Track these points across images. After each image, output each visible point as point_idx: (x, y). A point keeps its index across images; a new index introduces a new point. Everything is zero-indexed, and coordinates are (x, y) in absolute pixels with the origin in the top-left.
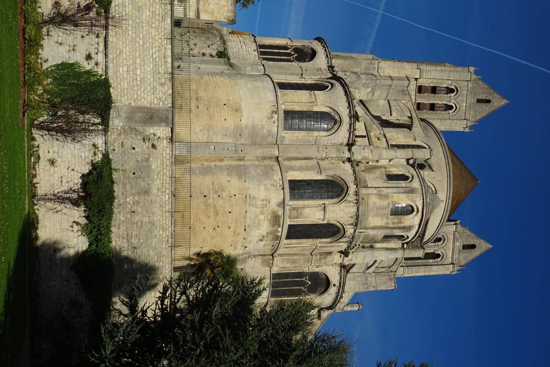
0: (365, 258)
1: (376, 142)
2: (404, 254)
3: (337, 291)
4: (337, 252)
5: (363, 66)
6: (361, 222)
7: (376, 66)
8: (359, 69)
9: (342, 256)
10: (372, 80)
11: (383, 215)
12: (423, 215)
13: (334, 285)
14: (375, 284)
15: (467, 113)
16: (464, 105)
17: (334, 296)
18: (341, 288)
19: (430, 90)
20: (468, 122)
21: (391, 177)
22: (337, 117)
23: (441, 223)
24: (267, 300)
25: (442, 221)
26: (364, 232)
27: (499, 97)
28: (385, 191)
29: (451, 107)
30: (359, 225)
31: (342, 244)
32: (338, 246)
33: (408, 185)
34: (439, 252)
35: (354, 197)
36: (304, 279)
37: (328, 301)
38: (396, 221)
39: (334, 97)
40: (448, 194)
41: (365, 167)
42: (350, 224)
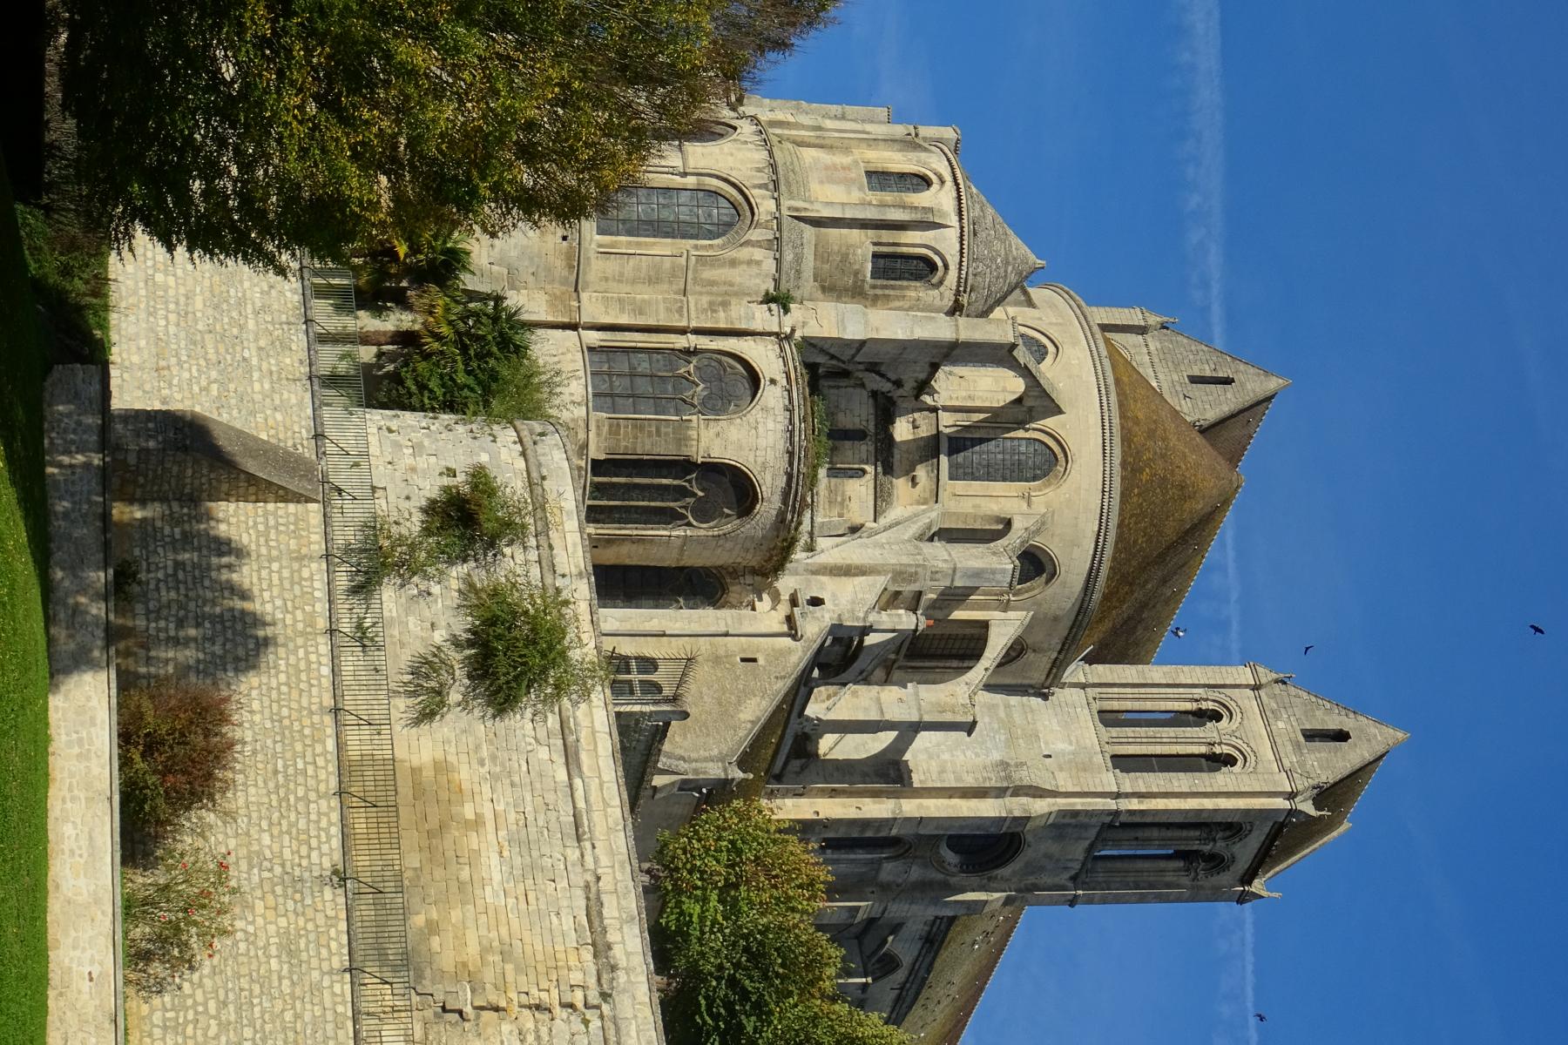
0: (843, 320)
2: (957, 326)
3: (787, 402)
4: (761, 303)
6: (788, 184)
9: (774, 306)
11: (848, 182)
12: (957, 184)
13: (773, 382)
14: (947, 557)
17: (782, 417)
18: (794, 384)
23: (1107, 431)
24: (584, 408)
25: (1107, 424)
26: (805, 209)
27: (1252, 370)
30: (783, 188)
31: (758, 254)
32: (750, 262)
34: (1226, 750)
35: (757, 138)
36: (682, 371)
37: (771, 440)
40: (1094, 349)
42: (760, 186)
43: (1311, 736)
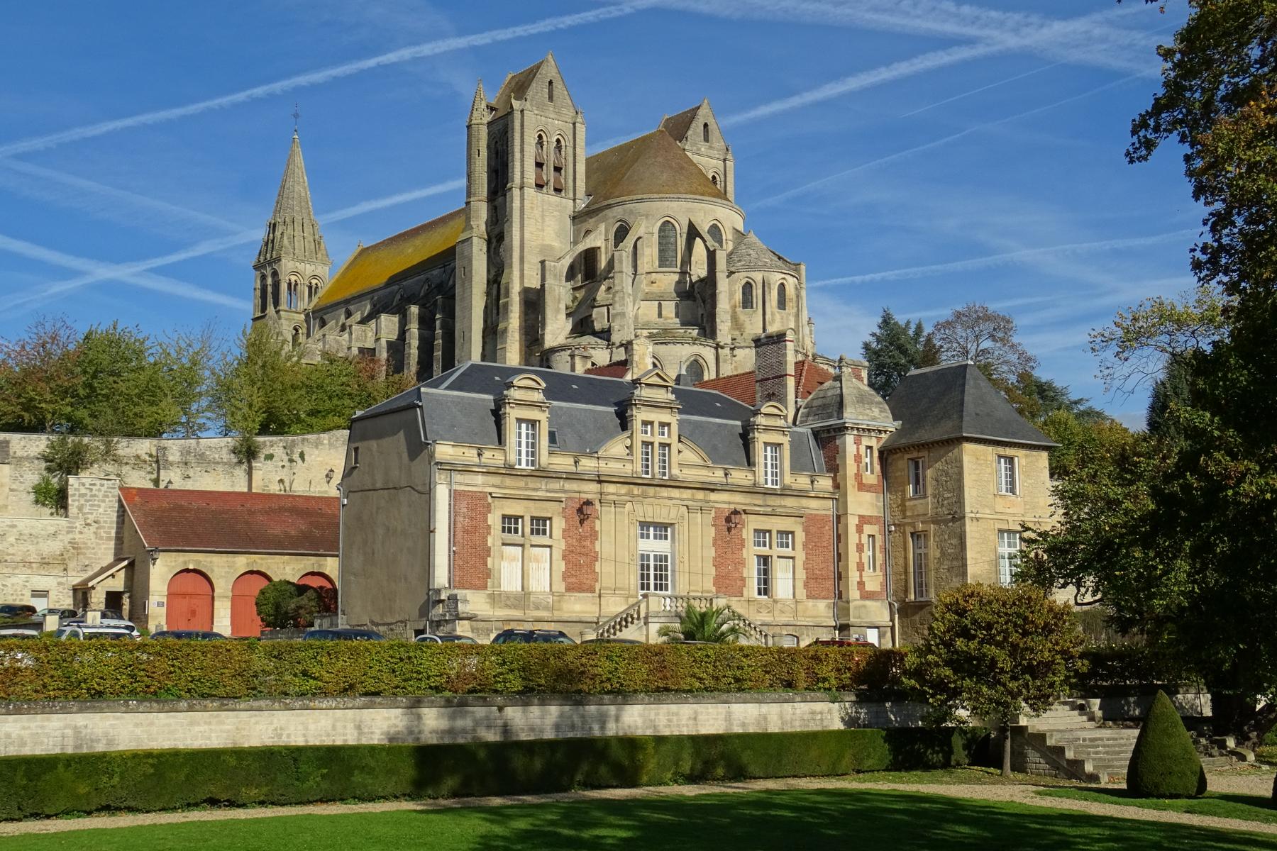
1: (658, 287)
5: (552, 282)
7: (553, 264)
8: (556, 287)
10: (623, 298)
15: (564, 119)
16: (556, 122)
19: (540, 169)
20: (578, 120)
21: (747, 302)
22: (692, 359)
28: (768, 316)
29: (558, 141)
33: (760, 286)
38: (791, 304)
39: (670, 358)
41: (734, 329)
43: (706, 139)
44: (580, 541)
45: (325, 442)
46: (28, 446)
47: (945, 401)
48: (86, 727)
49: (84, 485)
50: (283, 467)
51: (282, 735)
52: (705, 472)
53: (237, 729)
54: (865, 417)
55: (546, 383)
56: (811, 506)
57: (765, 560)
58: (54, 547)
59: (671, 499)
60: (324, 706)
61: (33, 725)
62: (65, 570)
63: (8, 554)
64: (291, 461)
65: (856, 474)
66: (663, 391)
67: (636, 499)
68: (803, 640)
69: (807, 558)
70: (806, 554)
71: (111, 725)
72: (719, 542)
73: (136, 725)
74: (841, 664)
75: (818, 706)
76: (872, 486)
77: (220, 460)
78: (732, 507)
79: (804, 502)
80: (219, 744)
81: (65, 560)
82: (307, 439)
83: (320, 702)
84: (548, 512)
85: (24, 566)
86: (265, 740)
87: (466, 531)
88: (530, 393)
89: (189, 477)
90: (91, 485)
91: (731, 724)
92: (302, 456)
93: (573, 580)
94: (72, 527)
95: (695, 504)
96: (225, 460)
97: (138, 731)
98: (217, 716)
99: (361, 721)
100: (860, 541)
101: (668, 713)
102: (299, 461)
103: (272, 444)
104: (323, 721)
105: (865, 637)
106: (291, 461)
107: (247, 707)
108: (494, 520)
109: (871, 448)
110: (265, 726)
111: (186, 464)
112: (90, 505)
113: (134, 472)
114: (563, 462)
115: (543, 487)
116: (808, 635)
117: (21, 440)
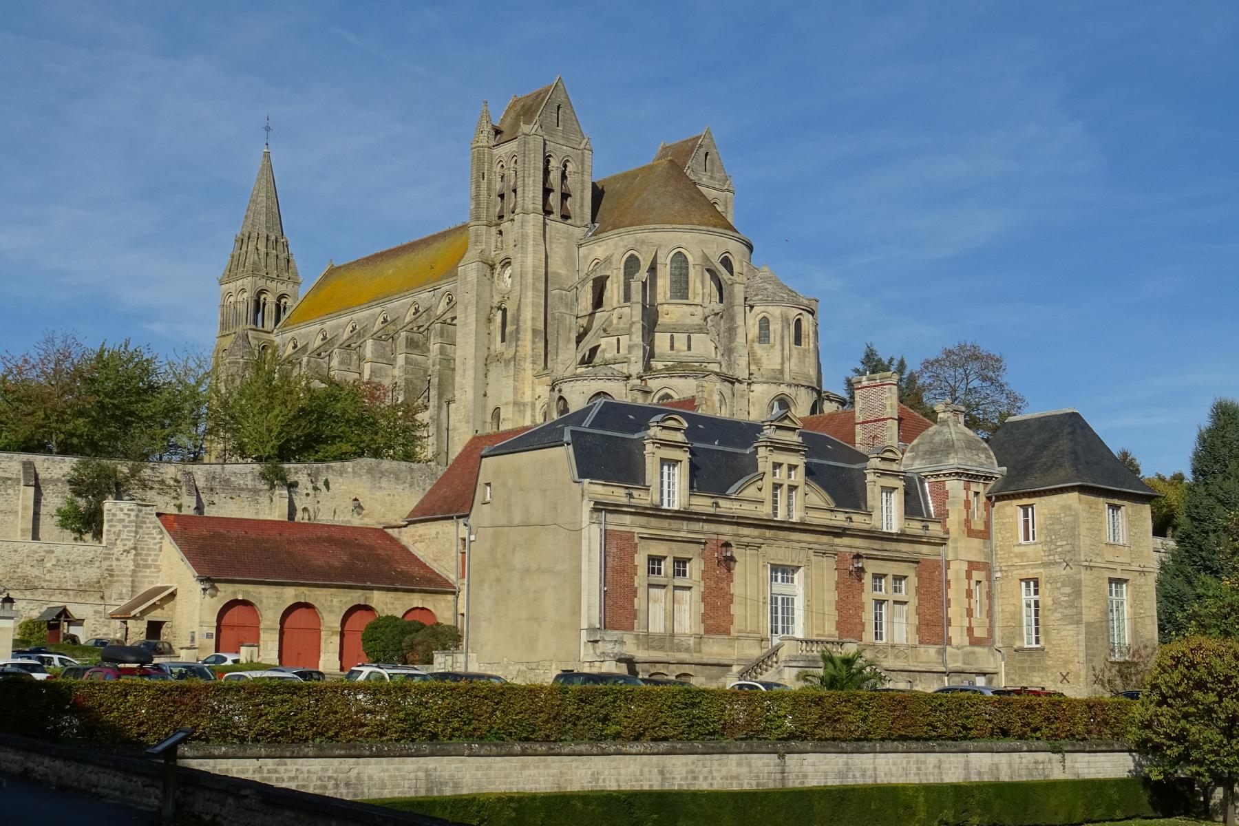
44: (717, 583)
45: (349, 470)
46: (52, 468)
47: (1053, 449)
48: (435, 769)
49: (121, 510)
50: (308, 495)
51: (599, 779)
52: (828, 515)
53: (561, 773)
54: (974, 464)
55: (688, 423)
56: (923, 552)
57: (879, 602)
58: (92, 573)
59: (799, 542)
60: (634, 751)
61: (391, 767)
62: (102, 598)
63: (45, 581)
64: (315, 489)
65: (965, 520)
66: (790, 433)
67: (768, 541)
68: (917, 685)
69: (919, 603)
70: (919, 599)
71: (456, 767)
72: (842, 586)
73: (478, 769)
74: (1051, 713)
75: (1041, 756)
76: (980, 532)
77: (245, 487)
78: (855, 551)
79: (918, 547)
80: (546, 788)
81: (101, 587)
82: (332, 467)
83: (630, 747)
84: (689, 553)
85: (61, 593)
86: (585, 785)
87: (615, 571)
88: (673, 433)
89: (214, 504)
90: (129, 510)
91: (969, 773)
92: (327, 484)
93: (711, 622)
94: (109, 554)
95: (820, 547)
96: (250, 487)
97: (479, 774)
98: (544, 761)
99: (663, 767)
100: (969, 587)
101: (918, 761)
102: (324, 489)
103: (298, 471)
104: (632, 766)
105: (974, 683)
106: (315, 489)
107: (571, 752)
108: (641, 560)
109: (977, 494)
110: (584, 771)
111: (212, 490)
112: (128, 531)
113: (159, 497)
114: (703, 504)
115: (685, 528)
116: (921, 681)
117: (44, 461)
